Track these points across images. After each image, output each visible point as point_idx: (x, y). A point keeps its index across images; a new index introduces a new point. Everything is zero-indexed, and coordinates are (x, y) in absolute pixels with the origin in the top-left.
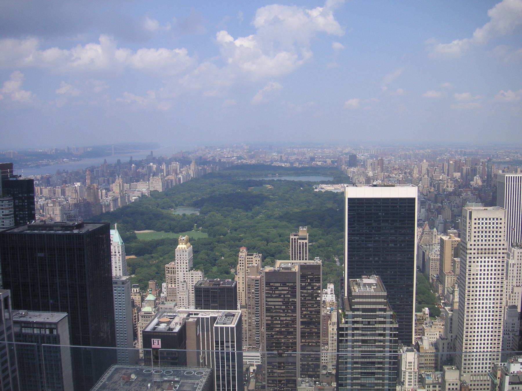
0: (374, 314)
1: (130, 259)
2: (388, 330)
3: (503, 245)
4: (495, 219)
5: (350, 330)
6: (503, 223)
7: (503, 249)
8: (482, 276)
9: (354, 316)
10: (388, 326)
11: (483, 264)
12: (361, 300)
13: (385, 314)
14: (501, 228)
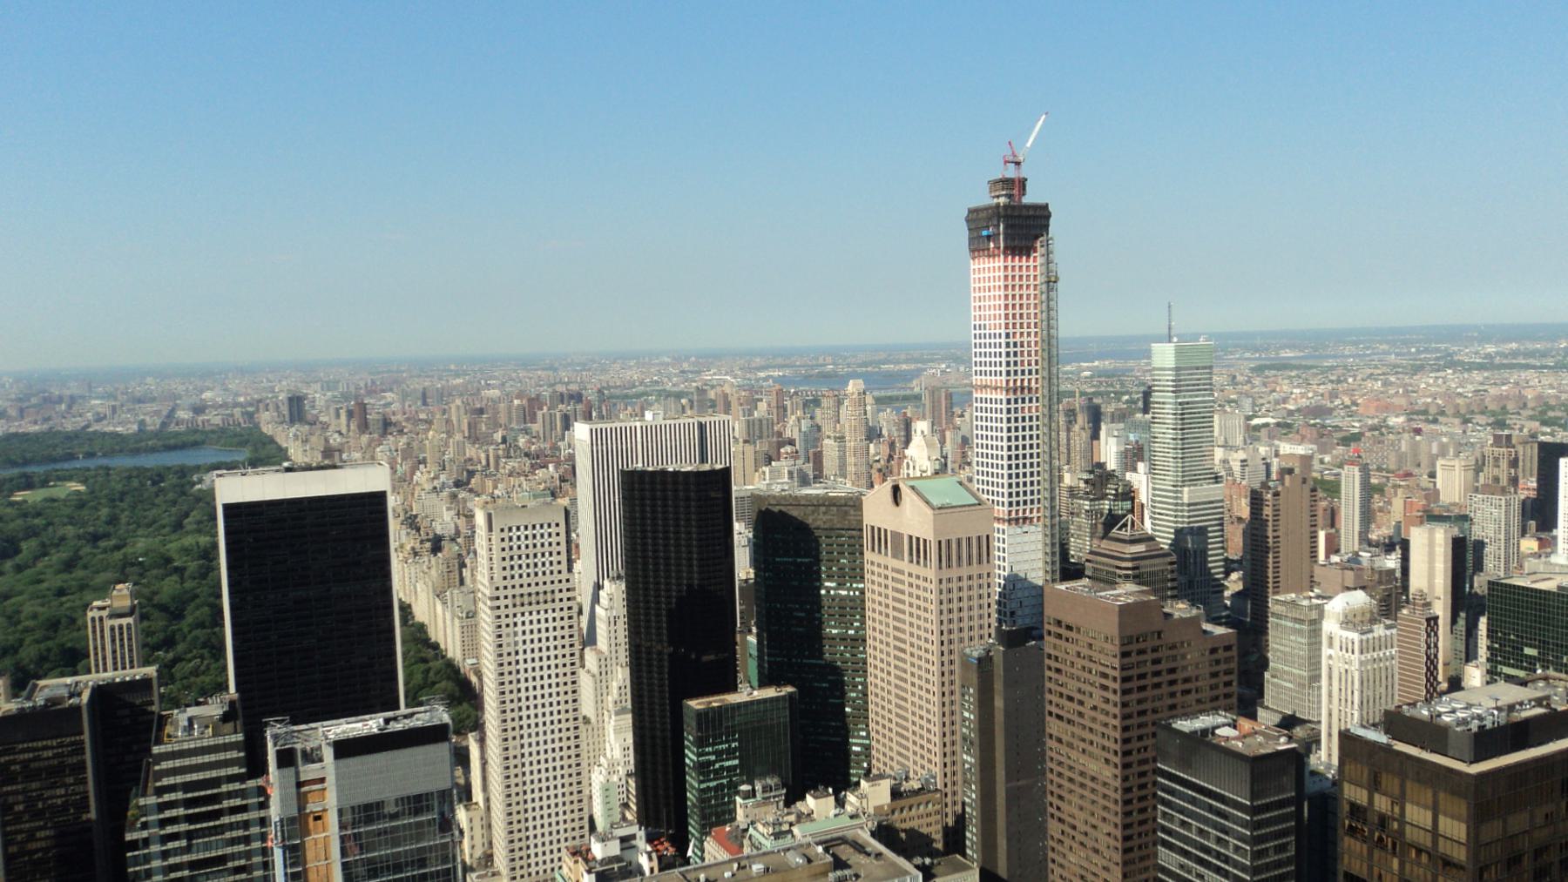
0: (215, 791)
2: (255, 825)
3: (568, 581)
4: (546, 526)
5: (154, 843)
6: (563, 534)
7: (568, 590)
8: (529, 656)
9: (163, 807)
10: (253, 815)
11: (528, 627)
12: (178, 763)
13: (243, 786)
14: (558, 544)
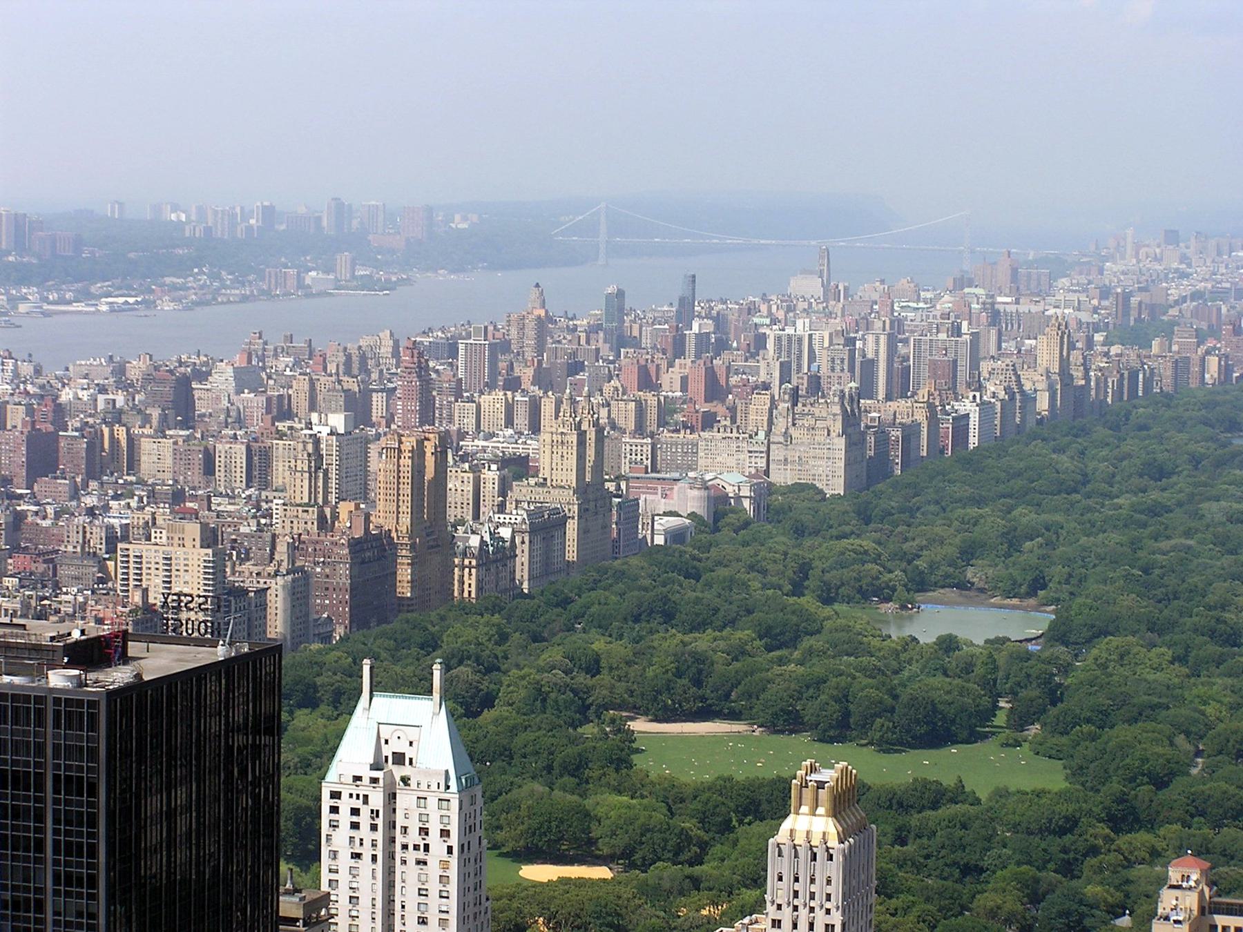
1: (564, 881)
